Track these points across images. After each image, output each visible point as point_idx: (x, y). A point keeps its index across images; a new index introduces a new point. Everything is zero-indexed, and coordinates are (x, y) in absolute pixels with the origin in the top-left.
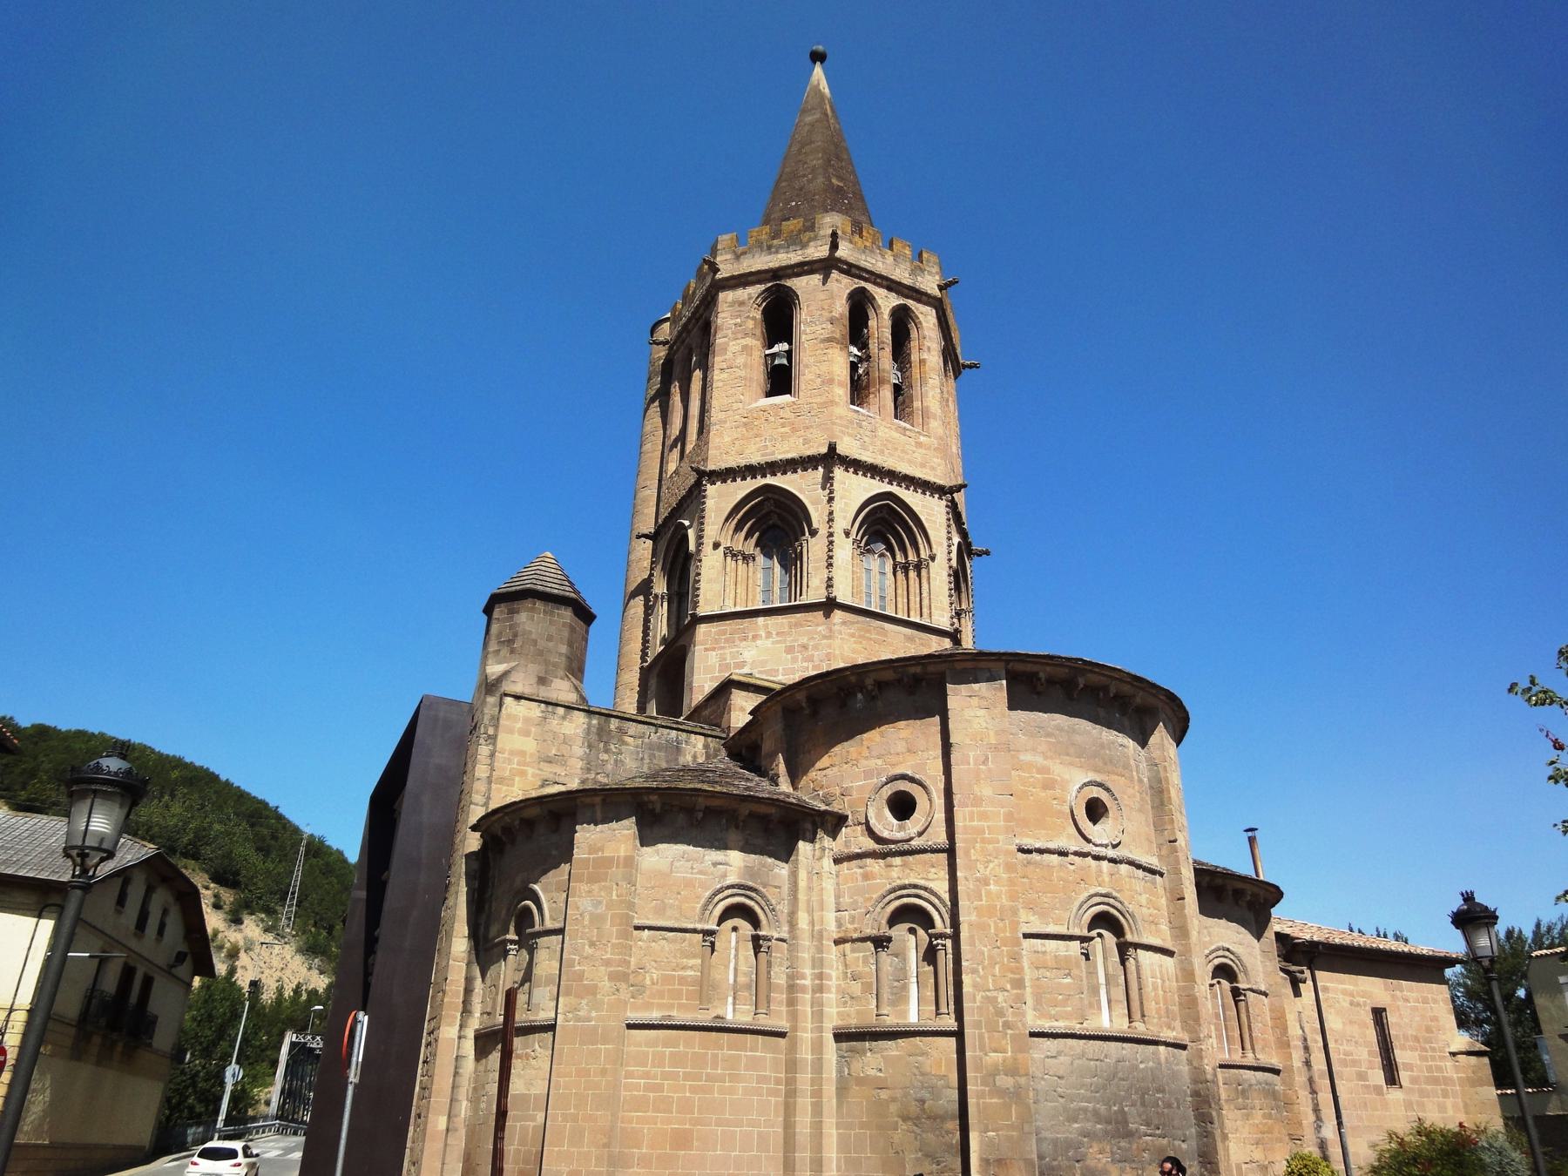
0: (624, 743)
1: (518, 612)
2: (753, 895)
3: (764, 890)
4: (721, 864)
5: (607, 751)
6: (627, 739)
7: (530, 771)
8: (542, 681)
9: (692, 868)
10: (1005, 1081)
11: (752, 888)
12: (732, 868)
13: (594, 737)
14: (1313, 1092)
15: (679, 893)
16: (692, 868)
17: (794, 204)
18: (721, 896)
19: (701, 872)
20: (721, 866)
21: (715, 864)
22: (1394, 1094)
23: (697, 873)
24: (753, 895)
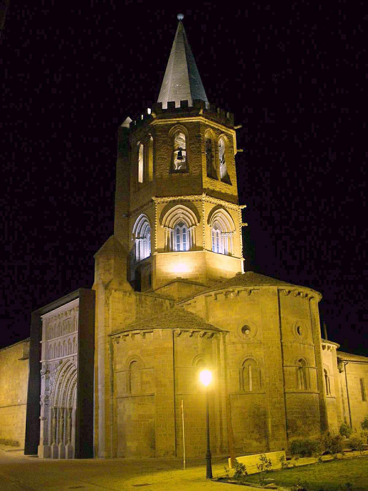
0: (146, 304)
1: (110, 260)
5: (142, 307)
6: (147, 303)
7: (122, 315)
8: (120, 284)
10: (277, 405)
13: (138, 303)
14: (343, 403)
17: (178, 85)
21: (195, 348)
22: (364, 403)
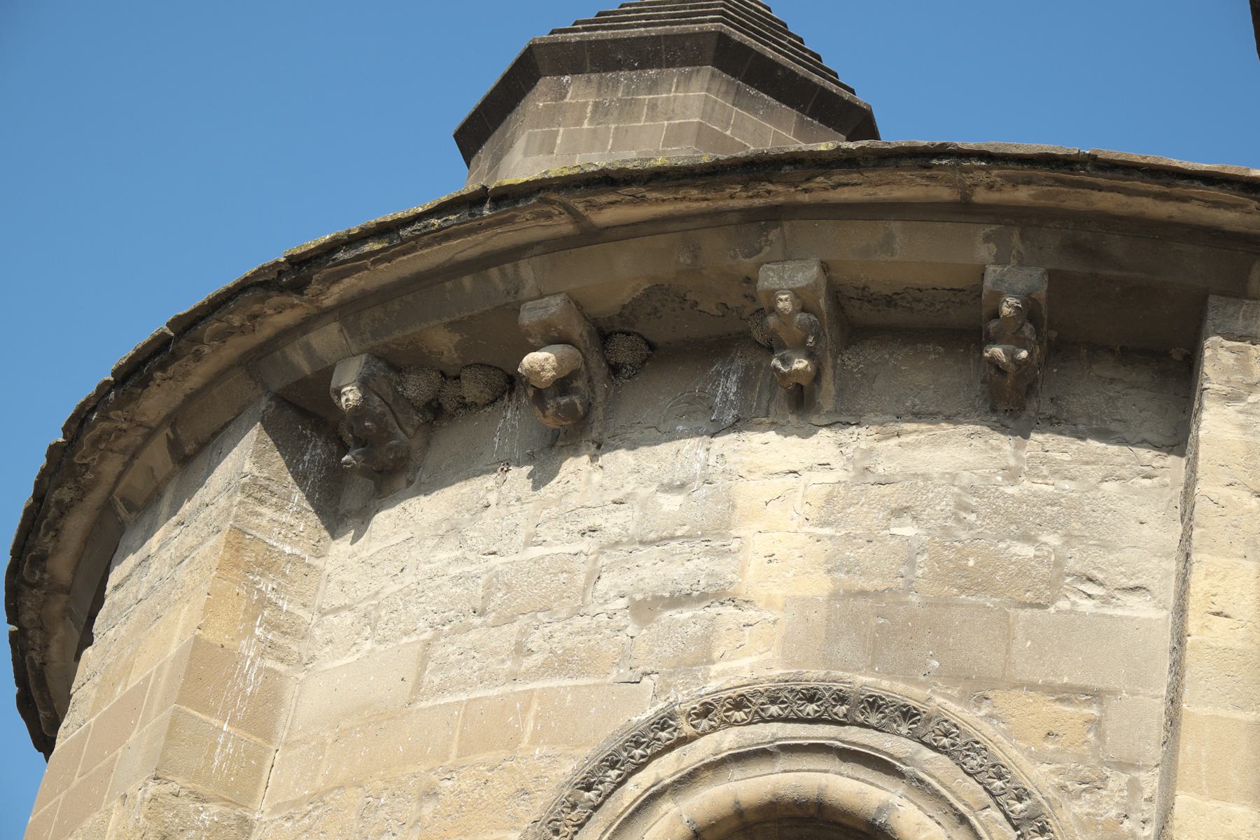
2: (893, 744)
3: (958, 712)
4: (678, 600)
9: (521, 650)
11: (874, 704)
12: (750, 614)
15: (431, 793)
16: (521, 650)
18: (665, 768)
19: (561, 664)
20: (685, 614)
23: (547, 669)
24: (893, 744)
